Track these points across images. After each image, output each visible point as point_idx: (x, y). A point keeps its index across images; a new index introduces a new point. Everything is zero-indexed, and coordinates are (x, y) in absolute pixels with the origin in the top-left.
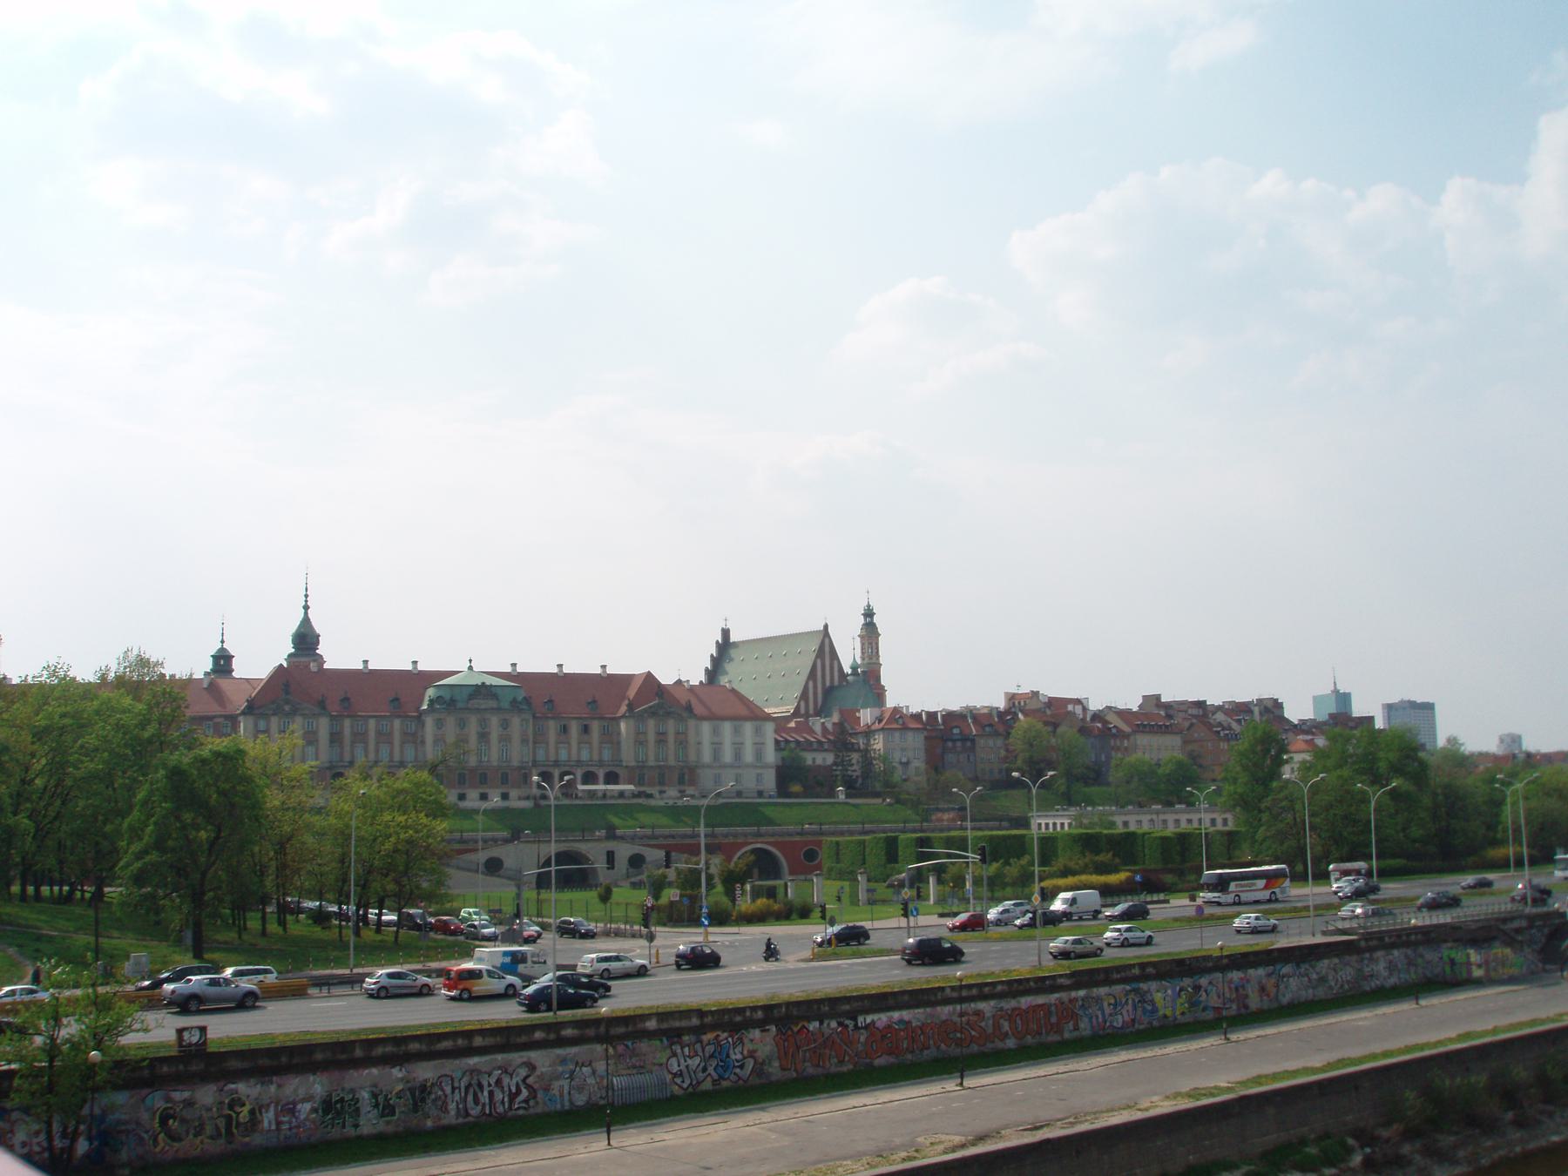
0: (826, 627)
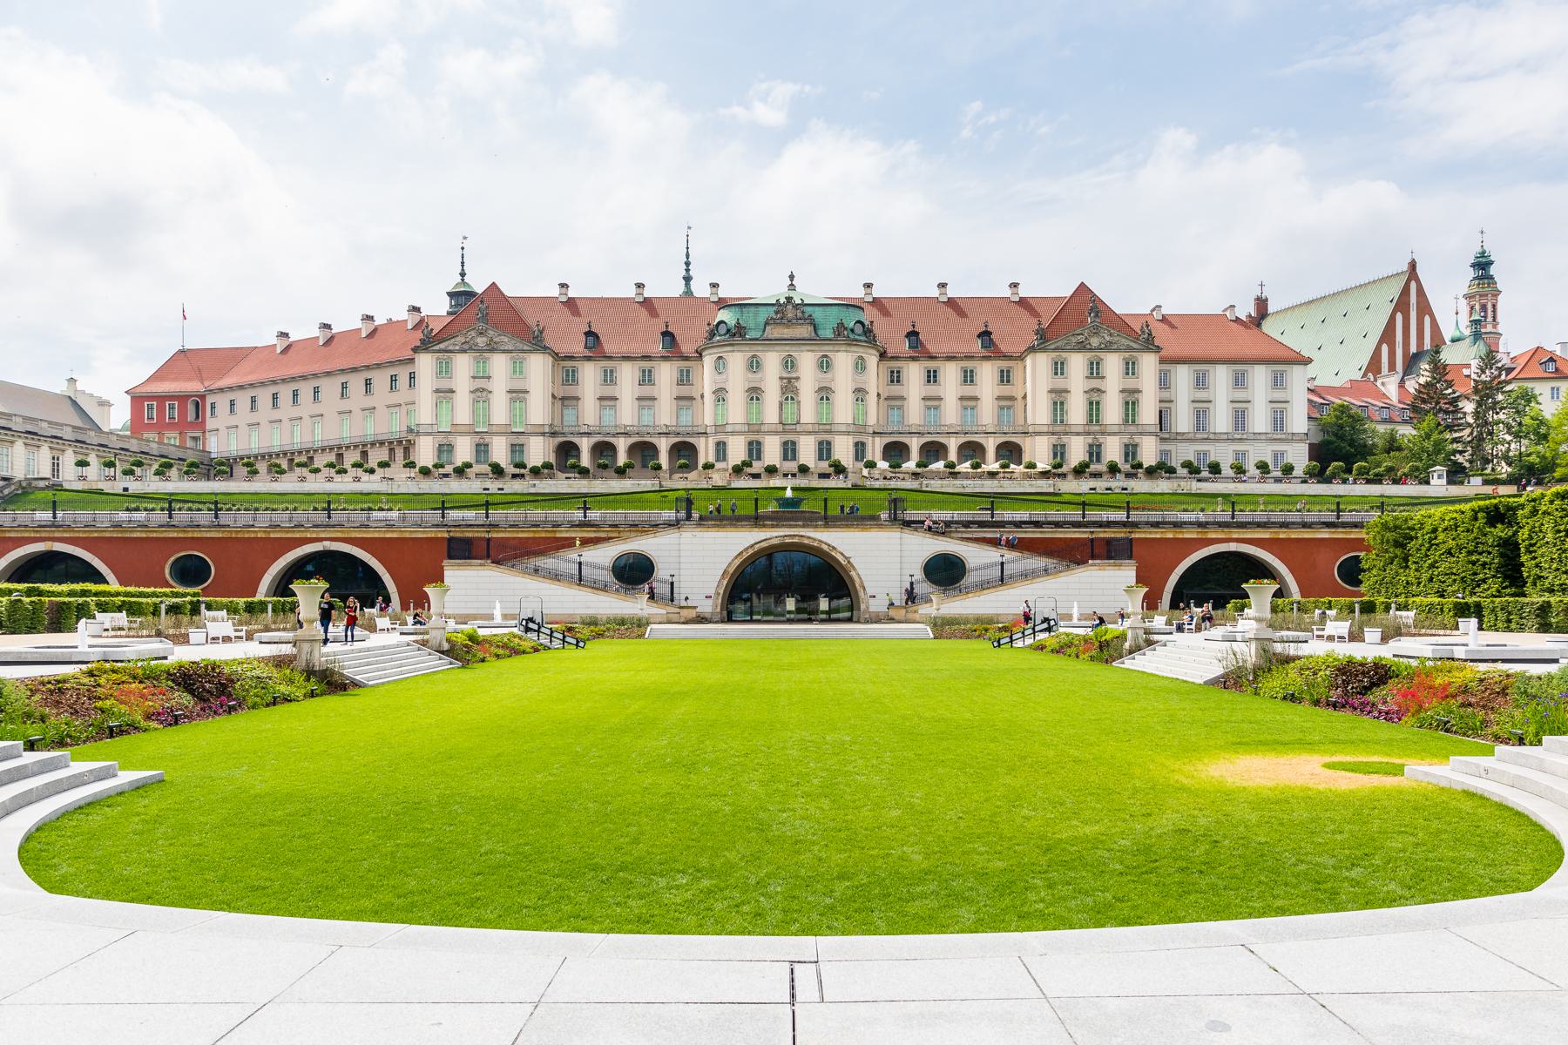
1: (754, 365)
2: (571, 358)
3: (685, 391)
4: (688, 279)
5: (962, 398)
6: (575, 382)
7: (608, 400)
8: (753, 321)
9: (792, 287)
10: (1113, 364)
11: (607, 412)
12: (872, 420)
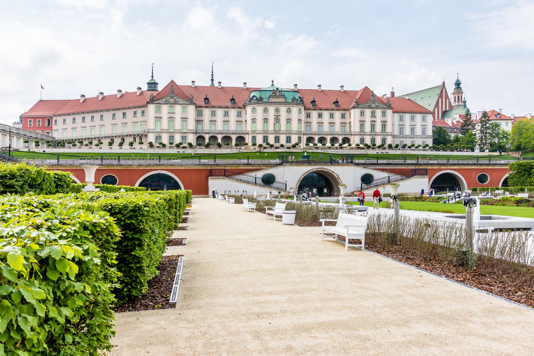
0: (444, 83)
1: (266, 111)
2: (201, 107)
3: (239, 119)
4: (212, 80)
5: (330, 123)
6: (202, 115)
7: (213, 122)
8: (265, 96)
9: (273, 85)
10: (379, 112)
11: (226, 126)
12: (303, 130)
